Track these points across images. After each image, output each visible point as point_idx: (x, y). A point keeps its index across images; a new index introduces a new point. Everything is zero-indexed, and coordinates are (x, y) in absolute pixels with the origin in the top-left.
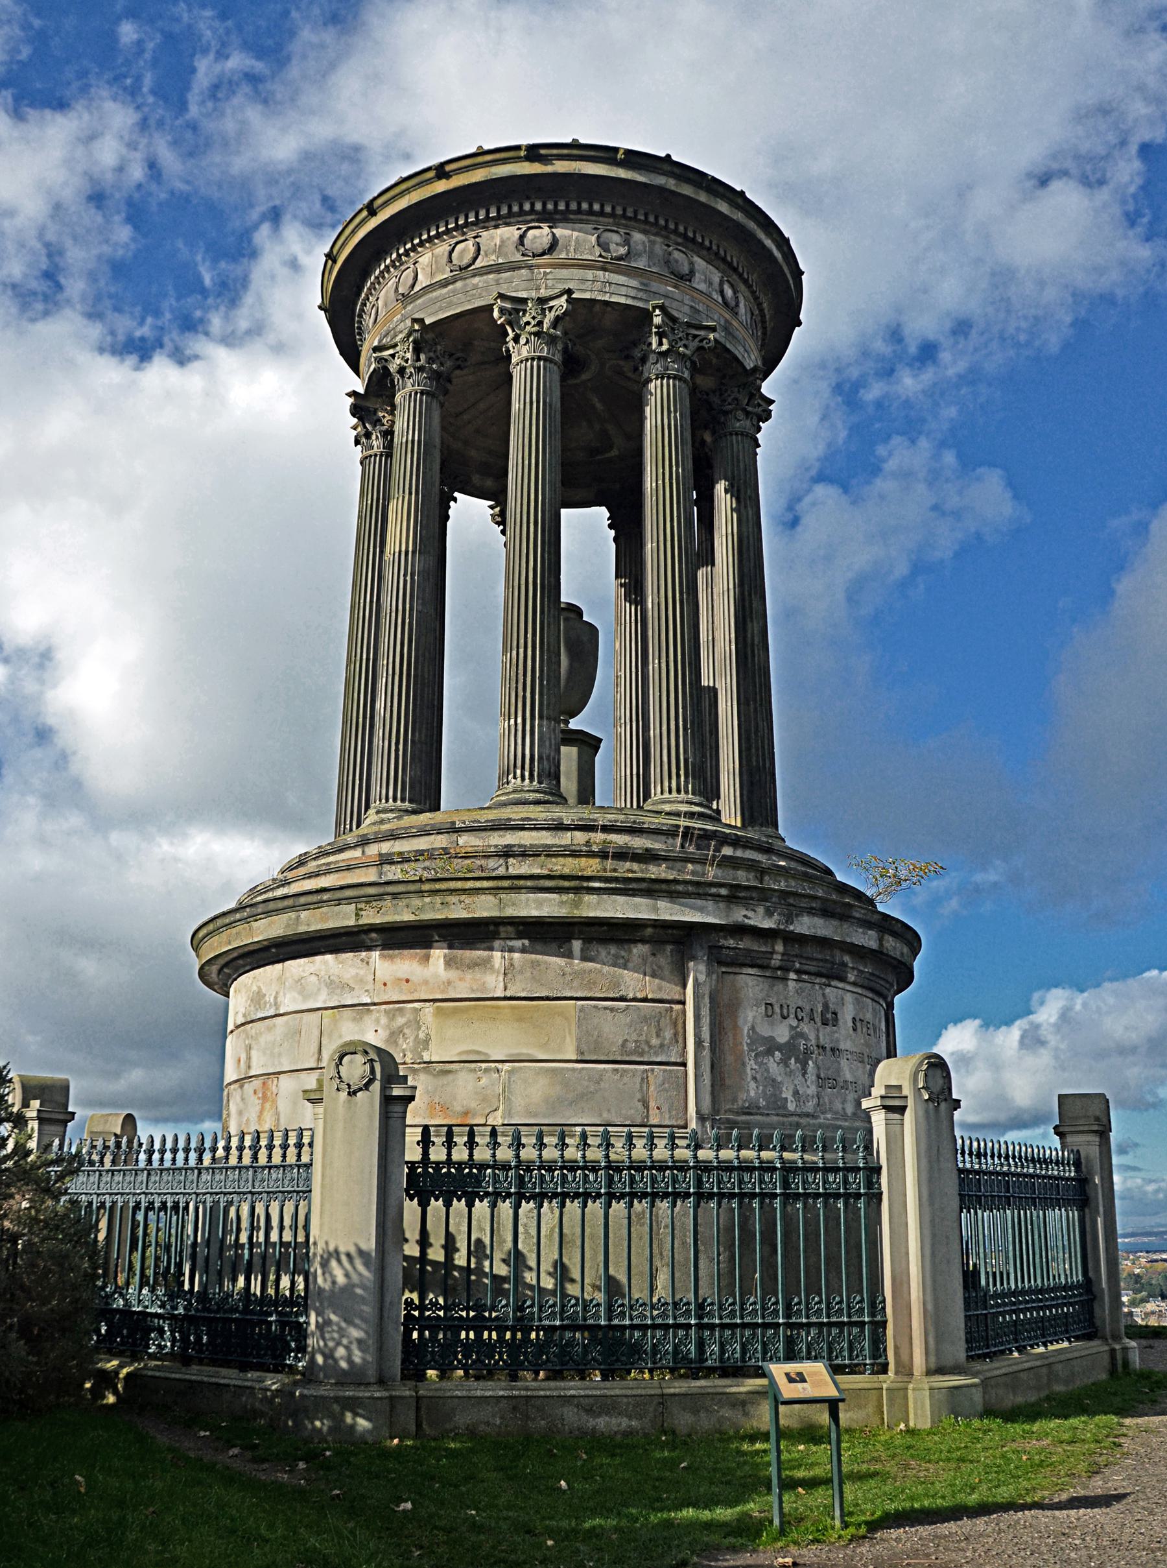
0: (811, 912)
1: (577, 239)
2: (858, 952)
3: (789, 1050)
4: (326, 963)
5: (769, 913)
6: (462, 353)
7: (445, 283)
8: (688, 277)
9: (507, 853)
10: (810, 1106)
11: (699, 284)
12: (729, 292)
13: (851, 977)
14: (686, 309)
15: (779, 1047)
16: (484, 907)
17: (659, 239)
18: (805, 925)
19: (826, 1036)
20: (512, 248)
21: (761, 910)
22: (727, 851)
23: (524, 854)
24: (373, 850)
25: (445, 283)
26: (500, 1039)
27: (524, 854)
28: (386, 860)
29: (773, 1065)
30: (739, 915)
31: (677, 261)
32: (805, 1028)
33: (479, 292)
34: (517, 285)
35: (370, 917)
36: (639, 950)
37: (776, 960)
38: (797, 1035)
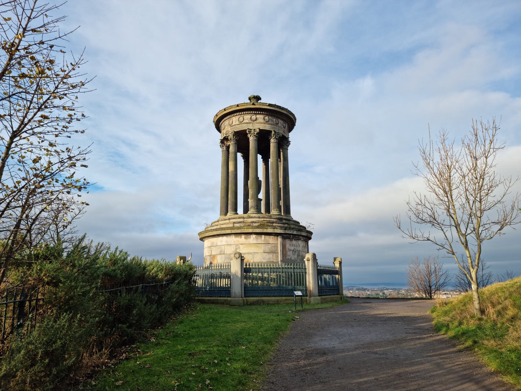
1: (260, 117)
2: (303, 236)
3: (293, 251)
4: (225, 238)
6: (241, 138)
7: (238, 125)
8: (278, 124)
9: (253, 222)
16: (250, 231)
18: (295, 233)
20: (249, 119)
22: (284, 221)
23: (255, 222)
24: (231, 221)
25: (238, 125)
26: (253, 250)
27: (255, 222)
28: (234, 223)
33: (243, 127)
34: (250, 126)
35: (233, 232)
36: (272, 237)
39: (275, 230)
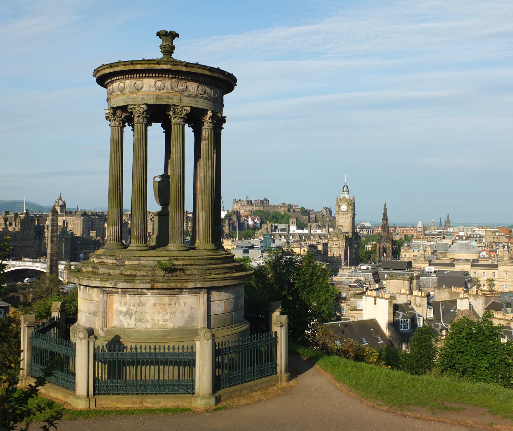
0: (122, 282)
5: (111, 283)
10: (132, 327)
11: (145, 89)
12: (159, 84)
13: (148, 294)
14: (140, 100)
15: (123, 313)
17: (132, 80)
19: (139, 309)
21: (109, 283)
29: (121, 317)
30: (103, 284)
31: (137, 85)
32: (131, 308)
36: (96, 290)
37: (120, 292)
38: (129, 310)
39: (90, 281)
